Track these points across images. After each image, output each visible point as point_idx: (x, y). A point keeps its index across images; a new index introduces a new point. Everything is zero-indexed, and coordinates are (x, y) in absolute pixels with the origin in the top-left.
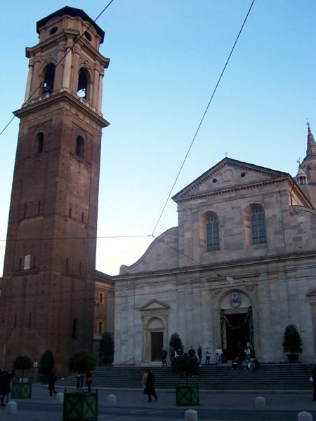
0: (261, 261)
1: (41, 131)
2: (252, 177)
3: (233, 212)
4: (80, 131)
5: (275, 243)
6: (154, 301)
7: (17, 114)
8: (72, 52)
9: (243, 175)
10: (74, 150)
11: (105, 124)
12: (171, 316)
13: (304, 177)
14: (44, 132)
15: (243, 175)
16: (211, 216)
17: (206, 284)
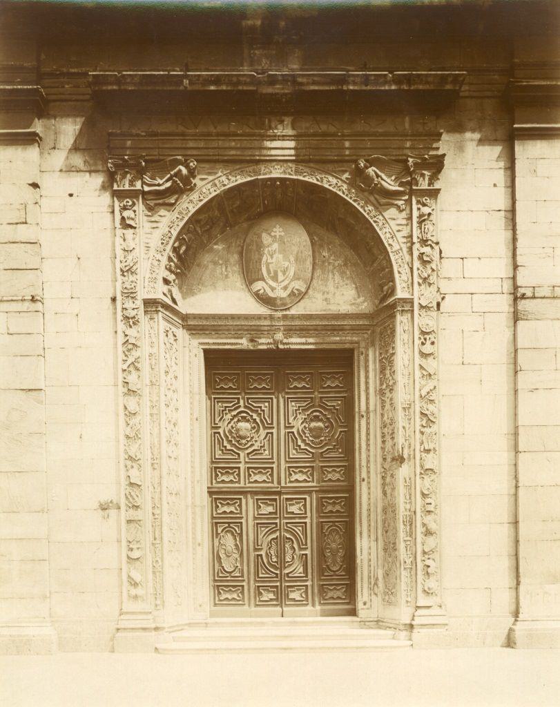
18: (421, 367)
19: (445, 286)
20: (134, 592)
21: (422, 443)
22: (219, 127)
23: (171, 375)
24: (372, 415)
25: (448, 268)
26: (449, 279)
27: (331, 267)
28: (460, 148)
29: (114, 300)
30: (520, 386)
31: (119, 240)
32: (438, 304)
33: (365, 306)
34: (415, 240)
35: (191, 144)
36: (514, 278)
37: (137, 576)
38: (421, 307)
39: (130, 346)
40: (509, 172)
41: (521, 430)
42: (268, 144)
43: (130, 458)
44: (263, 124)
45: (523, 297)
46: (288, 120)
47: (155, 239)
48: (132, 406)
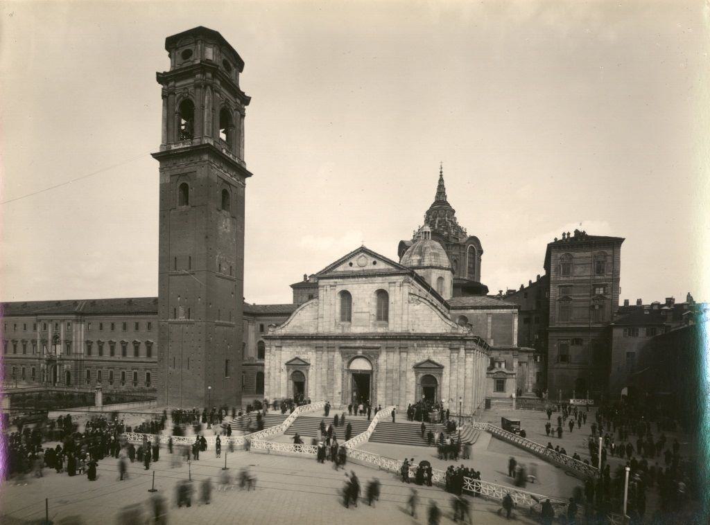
0: (384, 338)
1: (186, 182)
2: (381, 266)
3: (364, 294)
4: (225, 184)
5: (396, 324)
6: (297, 358)
7: (155, 156)
8: (212, 89)
9: (375, 263)
10: (219, 205)
11: (250, 175)
12: (310, 371)
13: (429, 232)
14: (189, 183)
15: (375, 263)
16: (346, 295)
17: (337, 350)
39: (343, 375)
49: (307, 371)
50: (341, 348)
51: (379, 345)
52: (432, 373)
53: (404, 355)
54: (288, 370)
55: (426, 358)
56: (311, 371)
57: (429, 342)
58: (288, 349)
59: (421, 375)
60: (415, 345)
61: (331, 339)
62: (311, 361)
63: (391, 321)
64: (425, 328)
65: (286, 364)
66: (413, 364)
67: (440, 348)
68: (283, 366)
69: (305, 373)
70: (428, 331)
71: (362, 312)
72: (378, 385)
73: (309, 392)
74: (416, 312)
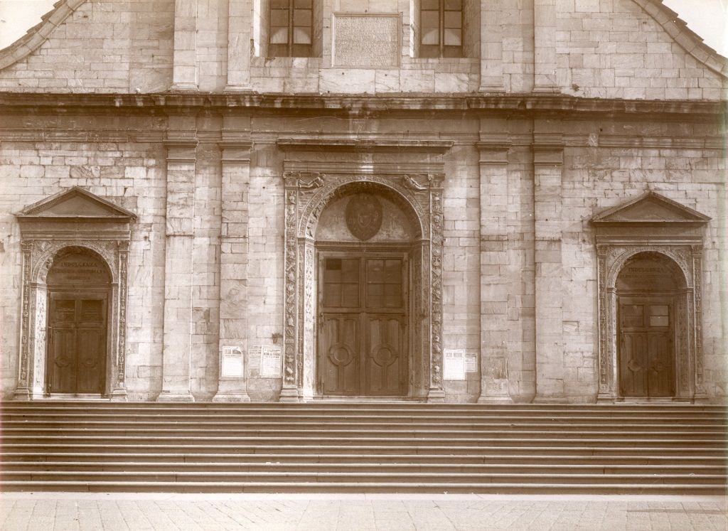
18: (433, 273)
19: (445, 233)
20: (288, 379)
21: (433, 309)
22: (337, 158)
23: (309, 272)
24: (411, 292)
25: (448, 225)
26: (448, 230)
27: (391, 219)
28: (454, 170)
29: (283, 237)
30: (482, 283)
31: (286, 210)
32: (442, 242)
33: (408, 238)
34: (431, 212)
35: (323, 166)
36: (480, 230)
37: (291, 372)
38: (433, 243)
39: (290, 260)
40: (478, 181)
41: (482, 303)
42: (360, 167)
43: (289, 314)
44: (358, 157)
45: (483, 240)
46: (370, 155)
47: (304, 209)
48: (291, 288)
49: (122, 248)
50: (282, 147)
51: (445, 139)
52: (666, 246)
53: (549, 179)
54: (26, 248)
55: (635, 192)
56: (141, 248)
57: (647, 129)
58: (30, 155)
59: (619, 256)
60: (593, 140)
61: (240, 111)
62: (141, 202)
63: (489, 48)
64: (623, 82)
65: (20, 220)
66: (586, 213)
67: (690, 153)
68: (12, 237)
69: (109, 257)
70: (633, 92)
71: (366, 15)
72: (446, 299)
73: (131, 337)
74: (585, 21)
